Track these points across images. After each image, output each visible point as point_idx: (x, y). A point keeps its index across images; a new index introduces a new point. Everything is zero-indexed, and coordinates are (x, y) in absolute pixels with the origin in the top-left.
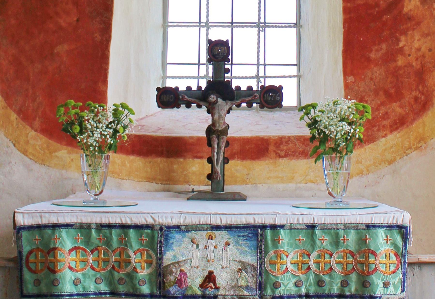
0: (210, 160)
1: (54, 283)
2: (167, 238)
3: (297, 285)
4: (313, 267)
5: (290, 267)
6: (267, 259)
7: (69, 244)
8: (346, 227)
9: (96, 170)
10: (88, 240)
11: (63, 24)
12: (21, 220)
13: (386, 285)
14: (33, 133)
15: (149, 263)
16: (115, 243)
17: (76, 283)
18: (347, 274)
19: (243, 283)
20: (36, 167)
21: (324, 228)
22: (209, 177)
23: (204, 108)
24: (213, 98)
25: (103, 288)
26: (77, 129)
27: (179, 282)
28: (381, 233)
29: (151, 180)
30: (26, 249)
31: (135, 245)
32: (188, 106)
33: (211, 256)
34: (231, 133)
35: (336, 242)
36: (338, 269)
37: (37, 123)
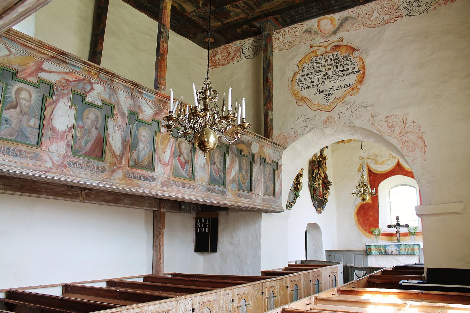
0: (397, 237)
1: (371, 252)
2: (386, 246)
3: (404, 252)
4: (406, 250)
5: (403, 250)
6: (400, 249)
7: (373, 248)
8: (411, 245)
9: (377, 238)
10: (375, 247)
11: (371, 214)
12: (367, 245)
13: (417, 253)
14: (367, 233)
15: (384, 250)
16: (379, 247)
17: (374, 252)
18: (411, 251)
19: (397, 252)
20: (368, 239)
21: (408, 245)
22: (397, 239)
23: (396, 228)
24: (396, 226)
25: (378, 253)
26: (373, 232)
27: (388, 252)
29: (388, 240)
30: (367, 248)
31: (382, 247)
32: (393, 227)
33: (392, 249)
34: (400, 232)
35: (409, 247)
36: (410, 250)
37: (368, 231)
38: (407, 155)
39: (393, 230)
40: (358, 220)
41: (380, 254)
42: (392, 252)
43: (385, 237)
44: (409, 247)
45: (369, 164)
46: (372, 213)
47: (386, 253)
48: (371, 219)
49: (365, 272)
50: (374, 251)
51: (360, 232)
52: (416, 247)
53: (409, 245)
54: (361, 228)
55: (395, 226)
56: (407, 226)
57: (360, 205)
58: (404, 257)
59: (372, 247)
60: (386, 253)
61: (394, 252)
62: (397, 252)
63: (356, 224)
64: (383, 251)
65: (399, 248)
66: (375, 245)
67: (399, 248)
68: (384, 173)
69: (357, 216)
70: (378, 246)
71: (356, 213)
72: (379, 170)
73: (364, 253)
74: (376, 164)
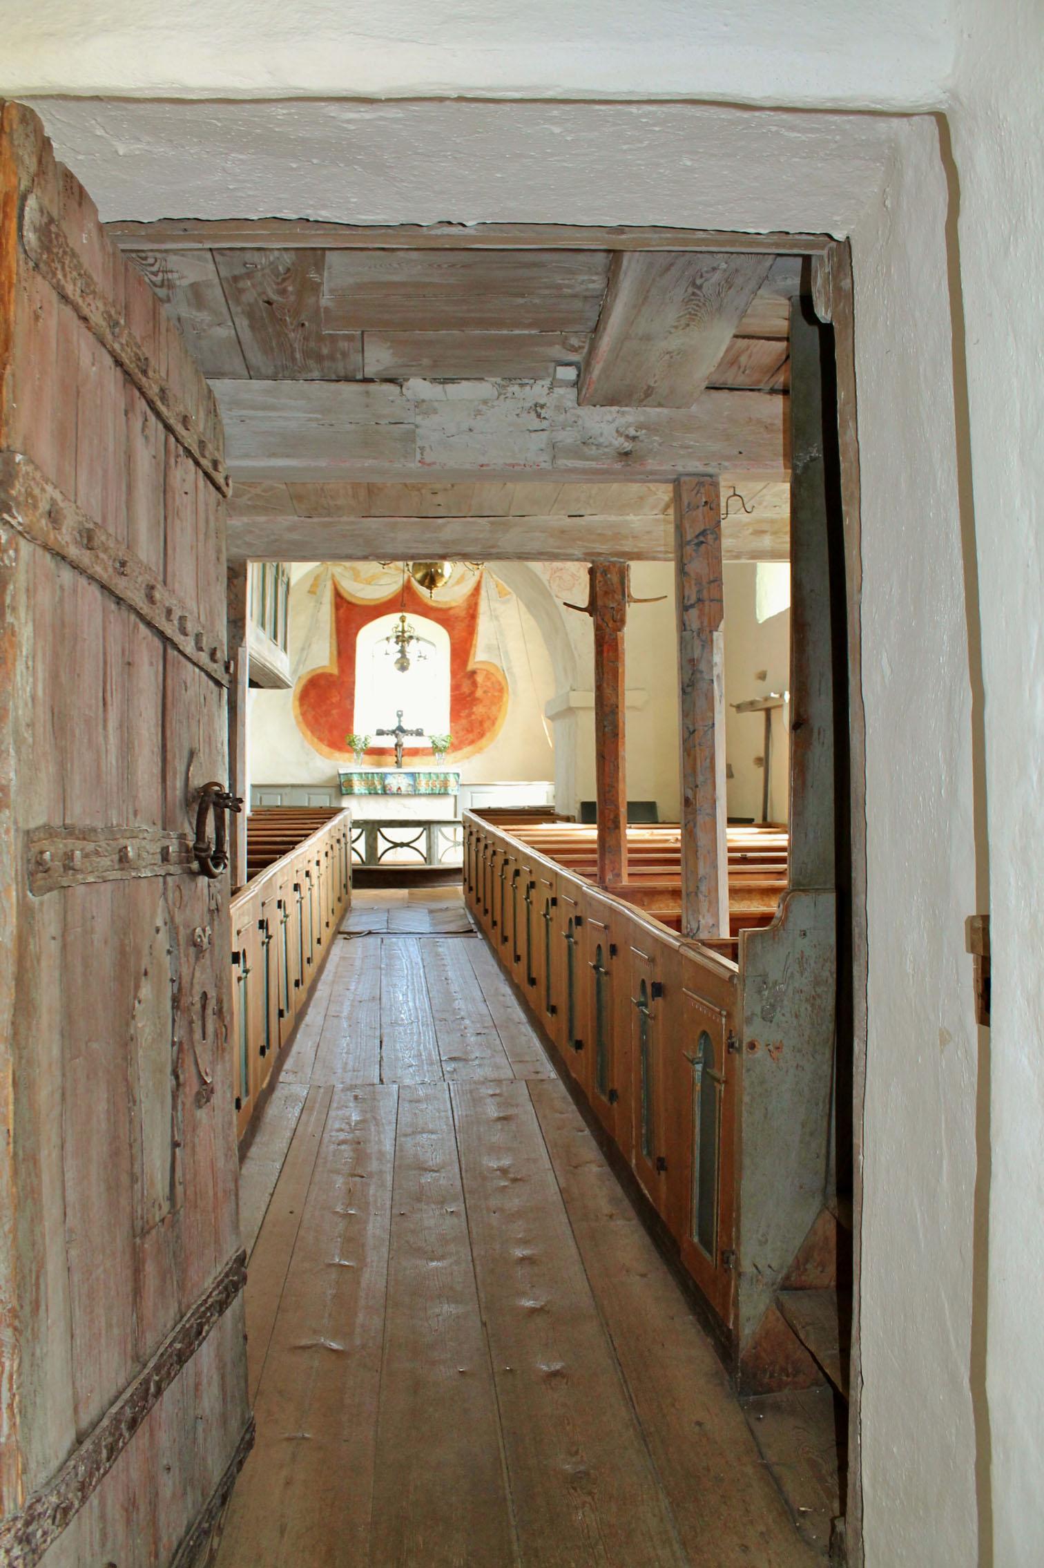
12: (341, 772)
20: (327, 760)
28: (451, 776)
34: (404, 746)
35: (438, 777)
37: (326, 742)
38: (559, 595)
39: (388, 742)
40: (304, 714)
41: (372, 793)
42: (399, 788)
43: (367, 758)
44: (438, 777)
45: (338, 578)
46: (338, 698)
47: (385, 791)
48: (334, 712)
49: (359, 831)
50: (359, 787)
51: (306, 743)
52: (452, 779)
53: (437, 775)
54: (309, 733)
55: (393, 732)
56: (419, 733)
57: (309, 677)
58: (423, 800)
59: (355, 778)
60: (385, 791)
61: (403, 789)
62: (410, 789)
63: (298, 723)
64: (379, 787)
65: (415, 780)
66: (360, 774)
67: (415, 780)
68: (372, 603)
69: (301, 705)
70: (365, 777)
71: (298, 696)
72: (361, 595)
73: (332, 791)
74: (355, 580)
